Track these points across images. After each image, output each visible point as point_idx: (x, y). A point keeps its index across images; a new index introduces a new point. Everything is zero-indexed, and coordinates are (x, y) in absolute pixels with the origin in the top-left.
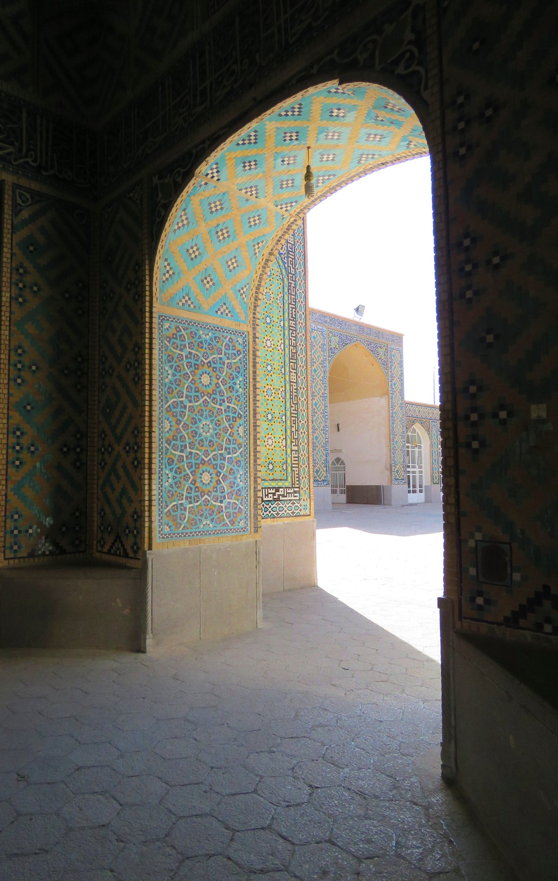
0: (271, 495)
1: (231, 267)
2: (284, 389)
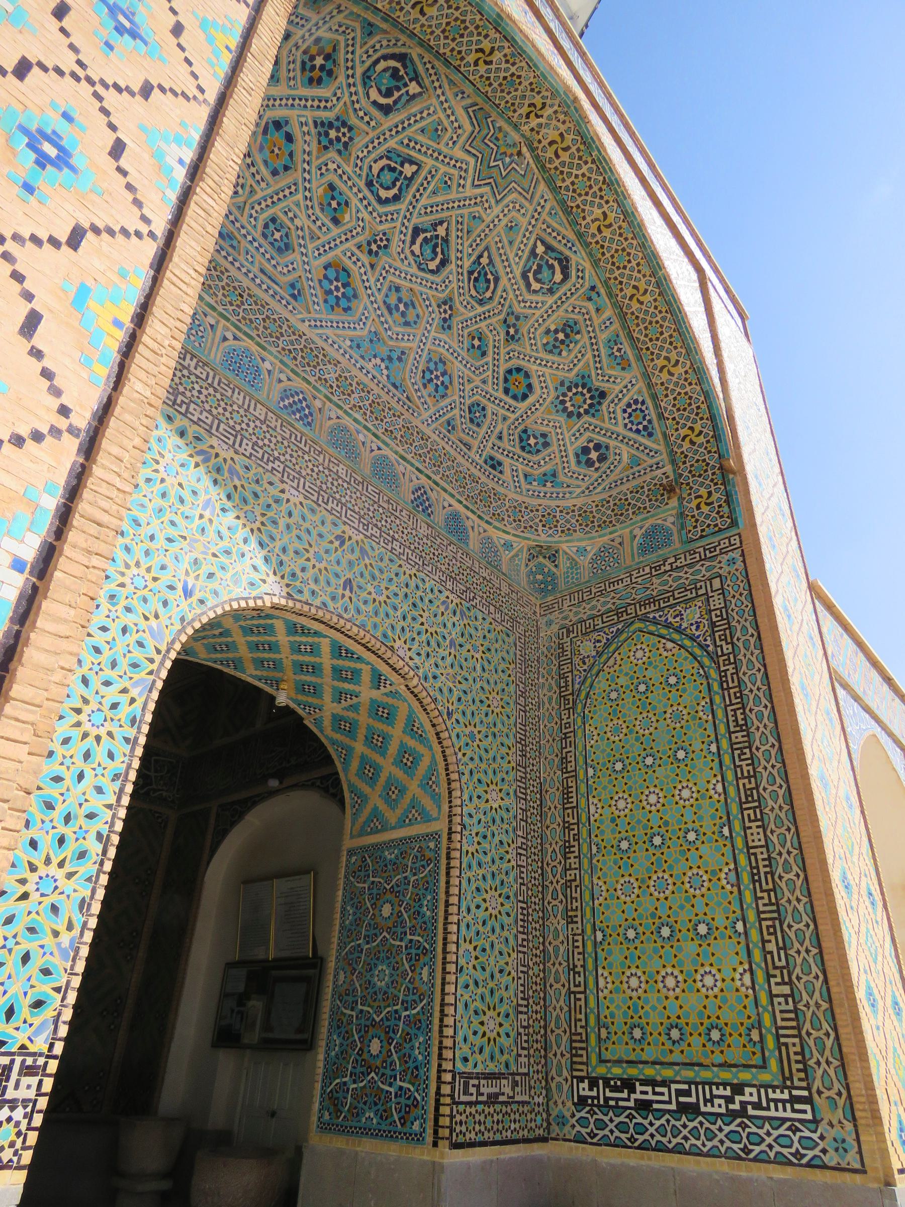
0: (722, 1101)
1: (409, 764)
2: (732, 866)
